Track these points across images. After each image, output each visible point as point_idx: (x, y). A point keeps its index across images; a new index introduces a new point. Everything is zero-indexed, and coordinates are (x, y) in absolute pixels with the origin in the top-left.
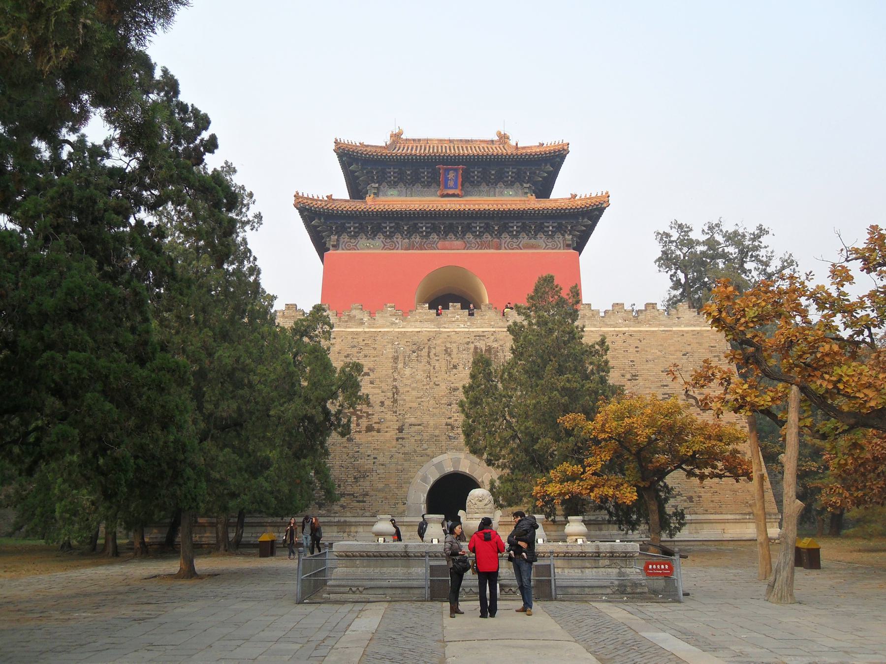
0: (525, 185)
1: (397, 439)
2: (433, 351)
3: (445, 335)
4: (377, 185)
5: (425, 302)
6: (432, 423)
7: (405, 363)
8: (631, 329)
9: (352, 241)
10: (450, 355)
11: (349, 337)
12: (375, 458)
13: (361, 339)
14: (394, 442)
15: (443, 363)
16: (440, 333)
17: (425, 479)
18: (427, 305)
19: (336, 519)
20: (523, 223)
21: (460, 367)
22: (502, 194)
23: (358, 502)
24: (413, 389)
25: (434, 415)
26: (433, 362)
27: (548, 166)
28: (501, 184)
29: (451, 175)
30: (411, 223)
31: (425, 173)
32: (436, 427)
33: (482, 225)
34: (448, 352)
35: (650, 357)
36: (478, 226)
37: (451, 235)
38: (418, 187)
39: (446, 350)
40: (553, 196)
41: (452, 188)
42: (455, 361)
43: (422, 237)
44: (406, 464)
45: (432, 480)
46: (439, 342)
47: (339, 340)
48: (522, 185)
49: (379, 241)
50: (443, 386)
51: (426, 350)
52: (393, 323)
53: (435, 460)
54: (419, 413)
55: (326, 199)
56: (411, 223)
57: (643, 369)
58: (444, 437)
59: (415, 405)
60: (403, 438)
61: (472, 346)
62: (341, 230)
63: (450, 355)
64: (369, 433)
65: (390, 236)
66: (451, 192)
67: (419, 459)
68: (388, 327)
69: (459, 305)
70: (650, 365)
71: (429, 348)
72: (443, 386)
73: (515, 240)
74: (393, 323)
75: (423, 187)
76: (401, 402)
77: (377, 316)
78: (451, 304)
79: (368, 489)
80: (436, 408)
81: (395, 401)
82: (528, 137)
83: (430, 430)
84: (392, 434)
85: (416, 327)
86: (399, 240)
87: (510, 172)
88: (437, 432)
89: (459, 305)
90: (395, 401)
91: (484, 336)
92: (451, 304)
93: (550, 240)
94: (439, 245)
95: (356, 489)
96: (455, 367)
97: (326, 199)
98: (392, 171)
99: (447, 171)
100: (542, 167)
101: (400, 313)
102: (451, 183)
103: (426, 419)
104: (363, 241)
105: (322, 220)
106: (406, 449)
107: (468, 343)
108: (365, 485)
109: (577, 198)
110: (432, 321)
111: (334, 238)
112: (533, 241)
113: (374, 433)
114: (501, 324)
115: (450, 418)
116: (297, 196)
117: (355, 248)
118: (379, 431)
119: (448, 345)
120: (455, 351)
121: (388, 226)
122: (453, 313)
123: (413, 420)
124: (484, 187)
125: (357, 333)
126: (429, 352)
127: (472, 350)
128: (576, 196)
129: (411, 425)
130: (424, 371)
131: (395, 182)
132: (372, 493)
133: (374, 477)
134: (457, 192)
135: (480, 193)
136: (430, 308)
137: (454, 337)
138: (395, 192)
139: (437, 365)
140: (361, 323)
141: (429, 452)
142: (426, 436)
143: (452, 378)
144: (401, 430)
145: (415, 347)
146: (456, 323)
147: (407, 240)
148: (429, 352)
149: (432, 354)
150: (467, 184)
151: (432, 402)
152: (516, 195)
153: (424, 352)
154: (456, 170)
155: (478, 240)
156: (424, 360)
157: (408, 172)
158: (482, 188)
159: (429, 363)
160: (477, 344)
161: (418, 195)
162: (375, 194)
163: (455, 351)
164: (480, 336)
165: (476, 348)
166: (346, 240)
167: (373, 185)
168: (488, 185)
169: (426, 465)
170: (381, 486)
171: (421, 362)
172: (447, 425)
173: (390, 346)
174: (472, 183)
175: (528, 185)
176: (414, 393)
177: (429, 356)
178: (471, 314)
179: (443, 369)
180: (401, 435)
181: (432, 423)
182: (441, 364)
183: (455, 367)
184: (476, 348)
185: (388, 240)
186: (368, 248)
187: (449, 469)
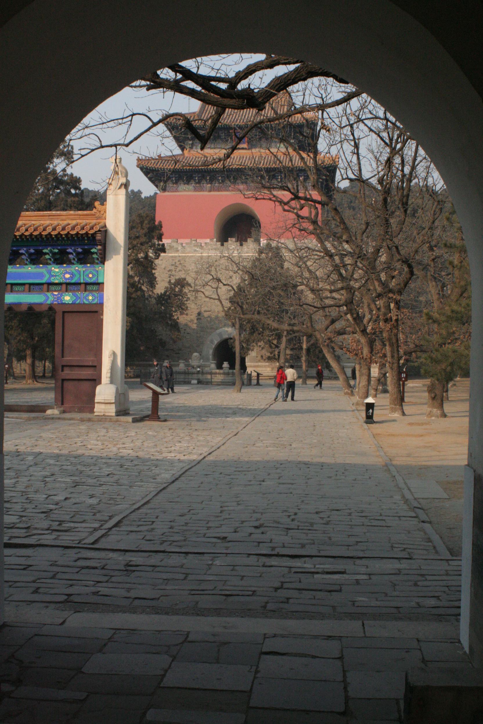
11: (170, 259)
12: (185, 330)
13: (177, 261)
17: (212, 341)
18: (215, 240)
43: (219, 183)
45: (216, 342)
47: (164, 261)
49: (191, 187)
52: (195, 251)
53: (218, 331)
54: (209, 305)
55: (157, 157)
65: (199, 183)
68: (192, 253)
76: (200, 298)
89: (234, 239)
97: (157, 157)
104: (182, 186)
116: (139, 160)
117: (177, 191)
122: (231, 244)
123: (206, 309)
125: (175, 257)
140: (177, 251)
147: (209, 185)
173: (194, 264)
178: (241, 245)
180: (199, 317)
185: (198, 185)
186: (185, 190)
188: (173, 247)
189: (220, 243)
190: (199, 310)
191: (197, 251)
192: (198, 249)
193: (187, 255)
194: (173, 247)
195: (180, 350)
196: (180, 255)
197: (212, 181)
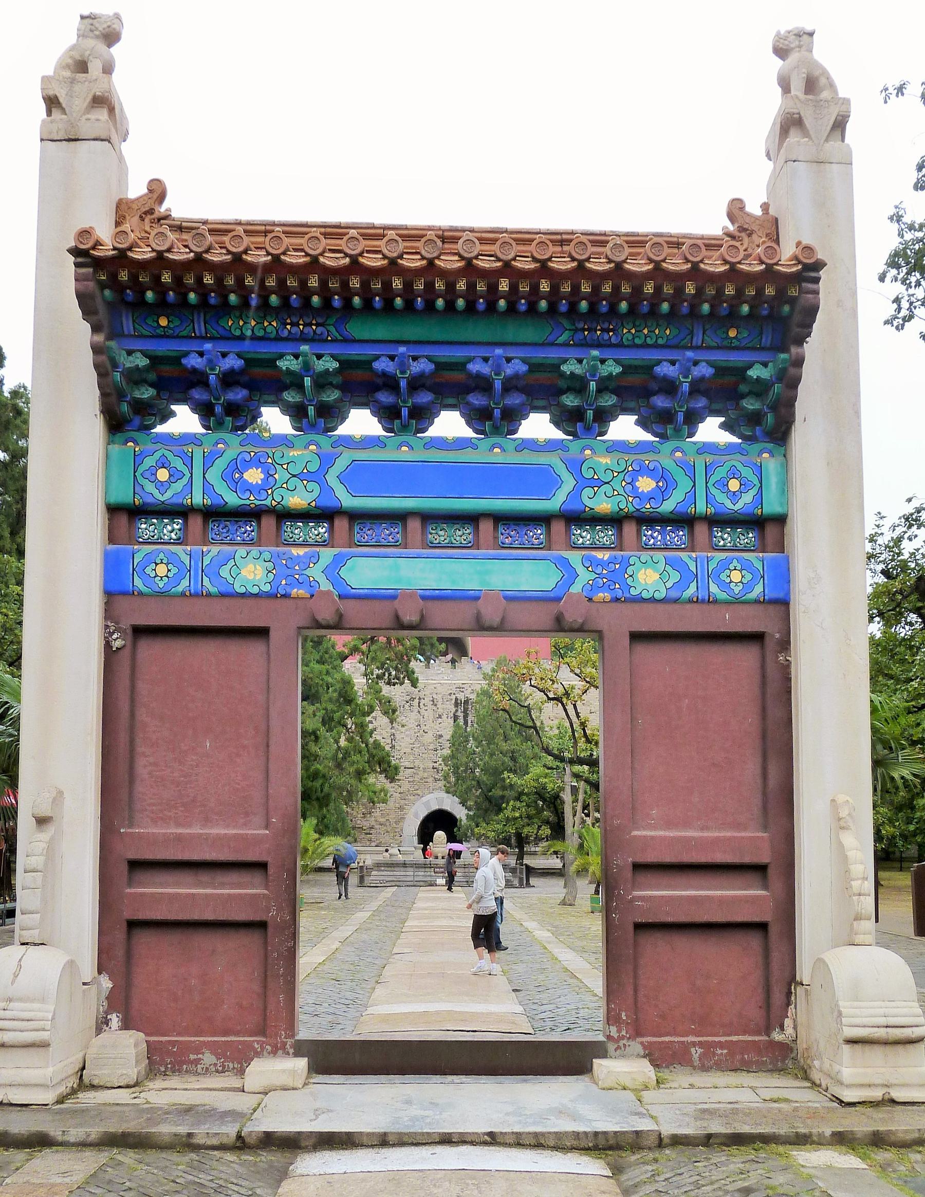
2: (422, 701)
15: (431, 712)
21: (444, 717)
23: (367, 834)
24: (407, 736)
26: (422, 711)
42: (440, 711)
50: (430, 734)
51: (417, 701)
58: (431, 779)
61: (453, 697)
71: (420, 699)
72: (430, 734)
79: (373, 823)
83: (421, 774)
88: (426, 775)
95: (366, 824)
96: (440, 717)
106: (401, 790)
114: (477, 677)
123: (407, 764)
127: (453, 701)
132: (377, 827)
137: (440, 689)
139: (426, 714)
143: (437, 727)
145: (408, 698)
156: (415, 712)
164: (461, 689)
165: (456, 699)
169: (417, 804)
170: (382, 820)
172: (433, 768)
181: (422, 766)
182: (429, 714)
183: (440, 717)
187: (435, 807)
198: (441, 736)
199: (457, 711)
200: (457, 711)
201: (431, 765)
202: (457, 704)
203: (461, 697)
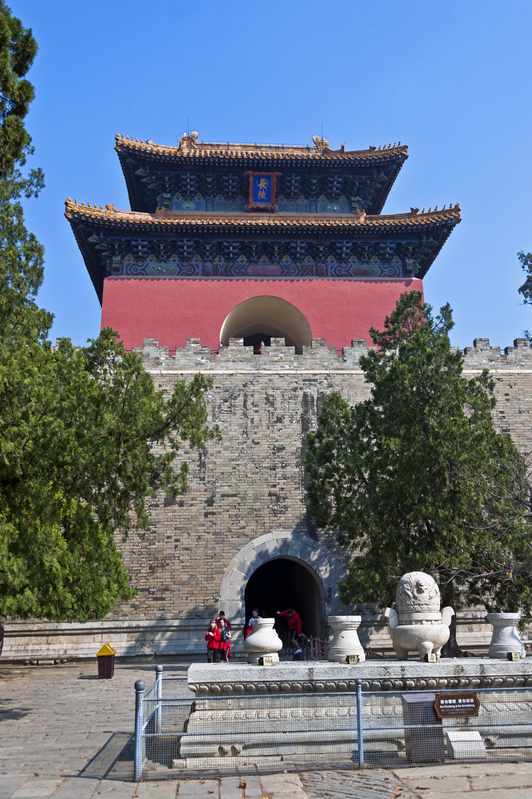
0: (353, 199)
1: (206, 515)
3: (266, 379)
4: (169, 195)
5: (238, 337)
6: (251, 492)
7: (214, 415)
8: (500, 371)
9: (140, 263)
10: (272, 404)
12: (177, 540)
14: (202, 519)
15: (264, 415)
16: (259, 376)
18: (242, 341)
19: (126, 624)
20: (354, 244)
21: (286, 421)
22: (324, 209)
23: (155, 599)
24: (226, 449)
25: (253, 482)
26: (251, 413)
27: (382, 175)
28: (322, 197)
29: (263, 184)
30: (215, 241)
31: (230, 180)
32: (256, 498)
33: (304, 245)
34: (269, 401)
35: (523, 407)
36: (300, 245)
37: (264, 258)
38: (220, 199)
39: (267, 399)
40: (383, 213)
41: (262, 200)
42: (279, 412)
44: (218, 548)
46: (258, 388)
48: (348, 198)
50: (264, 445)
51: (241, 398)
52: (198, 364)
53: (257, 542)
54: (234, 480)
56: (215, 241)
57: (516, 423)
58: (267, 512)
59: (229, 469)
60: (213, 514)
61: (300, 393)
62: (128, 249)
63: (272, 404)
64: (169, 508)
66: (262, 205)
67: (235, 540)
68: (191, 368)
69: (282, 340)
70: (524, 417)
71: (245, 396)
72: (264, 445)
73: (343, 265)
74: (198, 364)
75: (228, 198)
76: (211, 466)
77: (178, 355)
78: (272, 339)
79: (168, 582)
80: (256, 473)
81: (202, 465)
82: (354, 138)
84: (199, 508)
85: (227, 369)
86: (200, 264)
87: (337, 181)
88: (258, 505)
89: (282, 340)
90: (202, 465)
91: (316, 380)
92: (272, 339)
93: (386, 265)
94: (249, 270)
95: (154, 583)
96: (279, 420)
98: (189, 178)
99: (258, 178)
100: (376, 172)
101: (207, 350)
102: (262, 195)
103: (243, 487)
105: (102, 236)
106: (217, 528)
107: (295, 389)
108: (164, 576)
109: (419, 213)
110: (249, 361)
111: (117, 259)
112: (365, 266)
113: (176, 507)
115: (274, 486)
118: (181, 504)
119: (270, 392)
120: (279, 399)
121: (187, 244)
122: (276, 350)
123: (226, 490)
124: (302, 201)
126: (245, 401)
127: (300, 399)
128: (417, 210)
129: (223, 496)
130: (240, 425)
131: (191, 192)
132: (173, 587)
133: (177, 566)
134: (269, 206)
135: (297, 209)
136: (246, 344)
138: (192, 205)
139: (256, 418)
141: (247, 531)
142: (244, 510)
143: (276, 435)
144: (210, 502)
145: (227, 395)
146: (278, 364)
147: (208, 264)
148: (245, 401)
149: (249, 403)
150: (281, 197)
151: (251, 465)
152: (342, 211)
153: (240, 401)
154: (268, 178)
155: (298, 264)
156: (239, 412)
157: (209, 180)
158: (300, 201)
159: (245, 415)
160: (307, 390)
161: (221, 210)
162: (167, 206)
163: (279, 399)
164: (310, 381)
165: (305, 395)
166: (131, 262)
167: (165, 195)
168: (307, 198)
170: (185, 577)
171: (235, 414)
172: (270, 494)
174: (288, 196)
175: (358, 198)
176: (227, 454)
177: (245, 406)
179: (264, 423)
180: (210, 509)
181: (251, 492)
182: (260, 416)
183: (279, 420)
184: (305, 395)
188: (148, 355)
189: (252, 348)
190: (209, 495)
191: (202, 364)
192: (203, 361)
193: (180, 372)
194: (148, 355)
195: (166, 589)
196: (164, 372)
197: (214, 258)
198: (281, 449)
199: (306, 412)
200: (306, 412)
201: (266, 490)
202: (306, 401)
203: (313, 391)
